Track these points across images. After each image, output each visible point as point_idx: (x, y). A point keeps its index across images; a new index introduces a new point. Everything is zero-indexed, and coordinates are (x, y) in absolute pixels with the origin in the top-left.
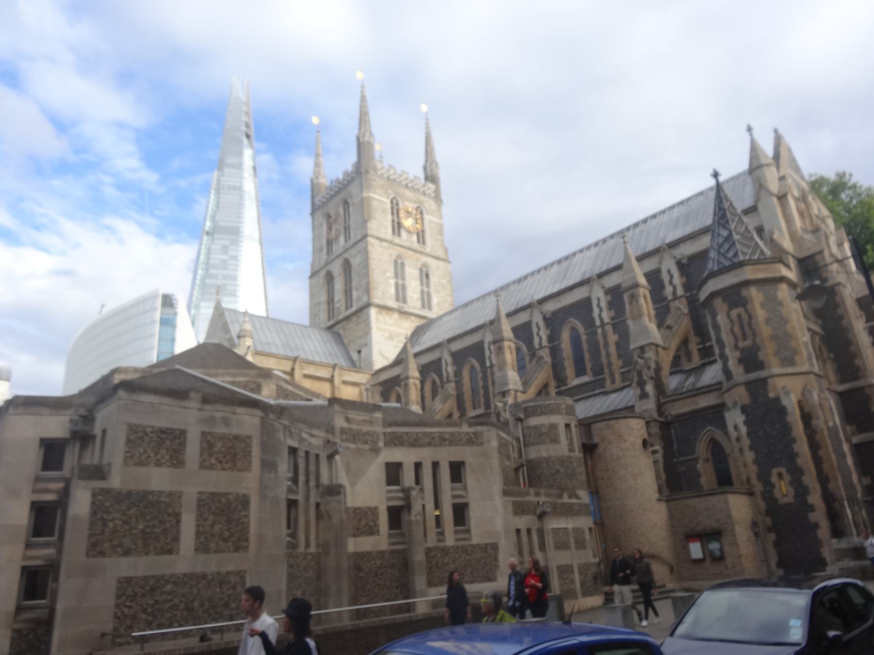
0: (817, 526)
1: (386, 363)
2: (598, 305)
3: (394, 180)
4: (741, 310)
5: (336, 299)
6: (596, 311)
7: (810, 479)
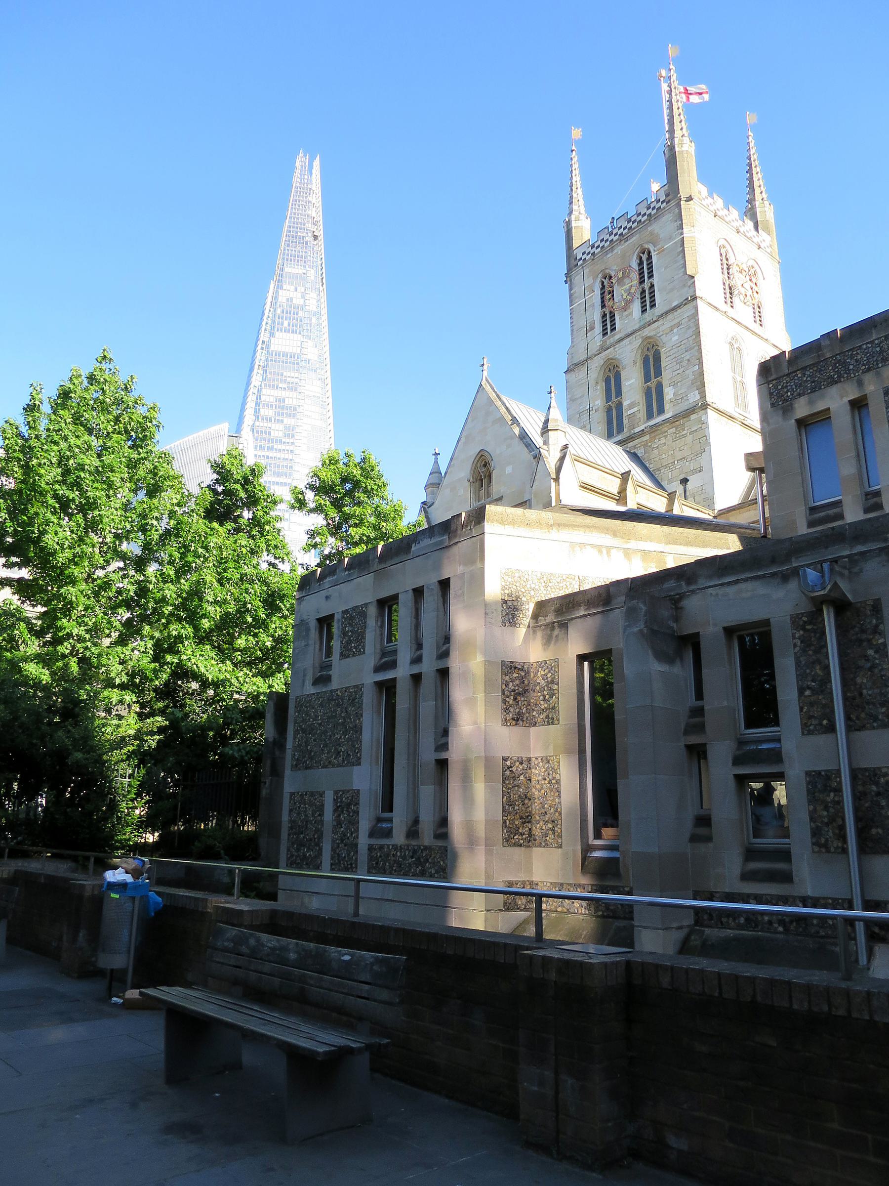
1: (735, 501)
5: (626, 403)
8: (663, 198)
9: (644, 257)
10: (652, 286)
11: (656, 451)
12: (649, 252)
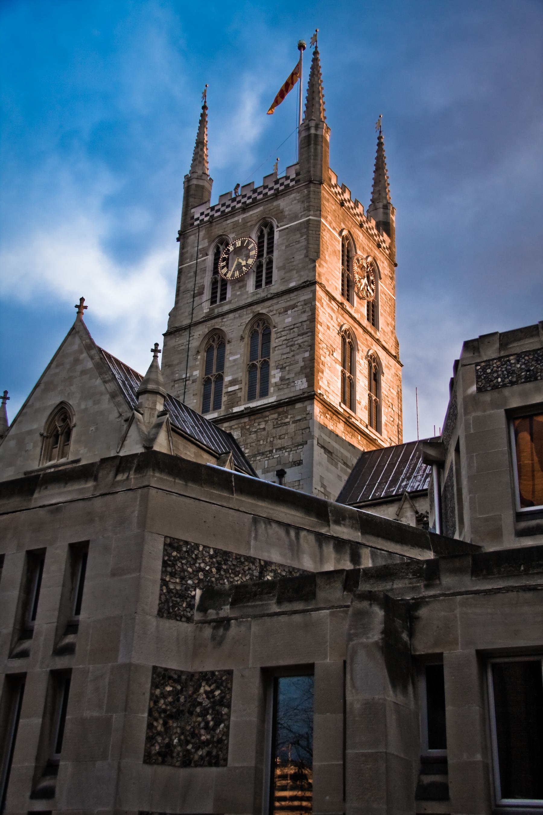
5: (227, 379)
8: (293, 176)
9: (266, 231)
11: (253, 436)
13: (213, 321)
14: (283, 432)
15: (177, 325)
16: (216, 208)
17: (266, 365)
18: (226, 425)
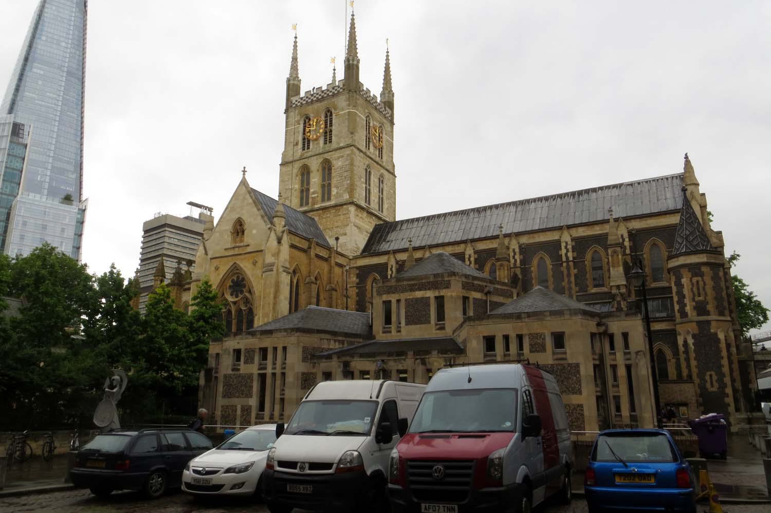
0: (729, 405)
2: (566, 247)
3: (369, 101)
4: (700, 279)
5: (311, 191)
6: (563, 251)
7: (727, 380)
8: (341, 86)
9: (329, 114)
10: (331, 131)
11: (324, 220)
12: (331, 113)
13: (304, 160)
14: (338, 219)
15: (286, 160)
16: (304, 99)
17: (329, 185)
18: (312, 213)
